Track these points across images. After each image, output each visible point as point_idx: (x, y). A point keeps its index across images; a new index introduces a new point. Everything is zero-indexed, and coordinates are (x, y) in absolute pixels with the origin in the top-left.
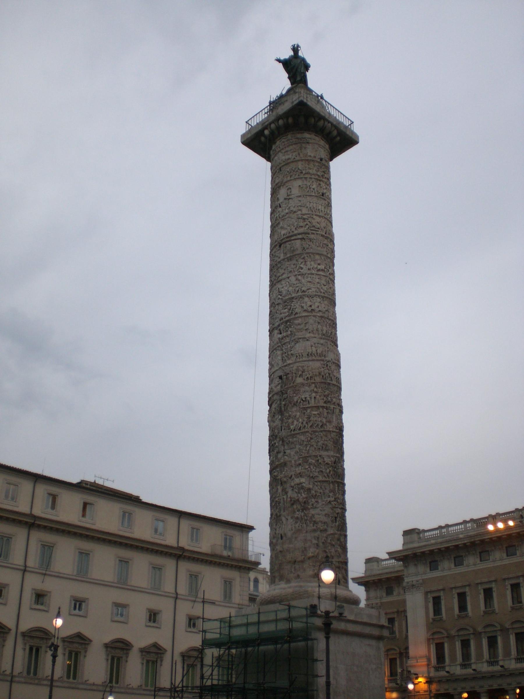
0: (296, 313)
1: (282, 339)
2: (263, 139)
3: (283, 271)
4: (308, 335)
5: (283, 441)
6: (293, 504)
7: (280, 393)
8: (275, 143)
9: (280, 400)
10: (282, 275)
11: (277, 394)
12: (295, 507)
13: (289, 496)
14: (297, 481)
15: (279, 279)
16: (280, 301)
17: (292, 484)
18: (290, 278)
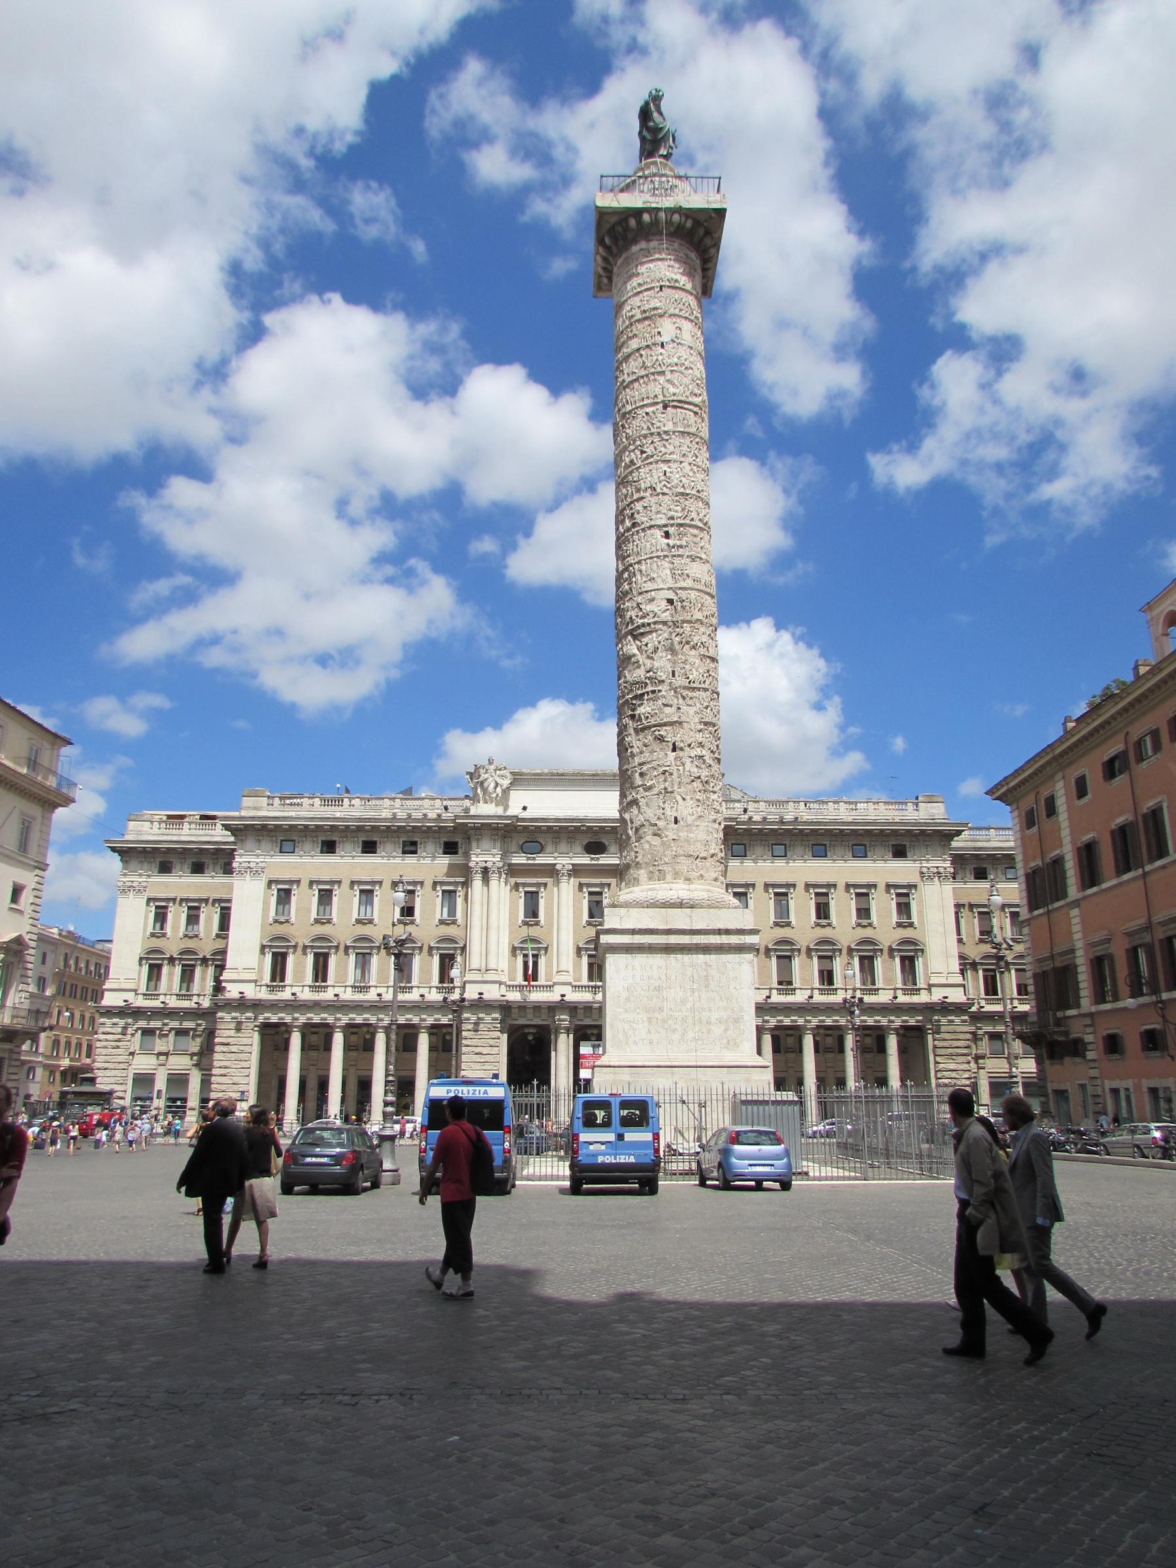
0: (692, 520)
1: (673, 547)
2: (632, 223)
3: (671, 448)
4: (703, 556)
5: (675, 692)
6: (693, 781)
7: (671, 624)
8: (648, 241)
9: (671, 633)
10: (670, 454)
11: (665, 623)
12: (694, 783)
13: (687, 769)
14: (698, 751)
15: (663, 458)
16: (665, 490)
17: (693, 755)
18: (683, 464)
